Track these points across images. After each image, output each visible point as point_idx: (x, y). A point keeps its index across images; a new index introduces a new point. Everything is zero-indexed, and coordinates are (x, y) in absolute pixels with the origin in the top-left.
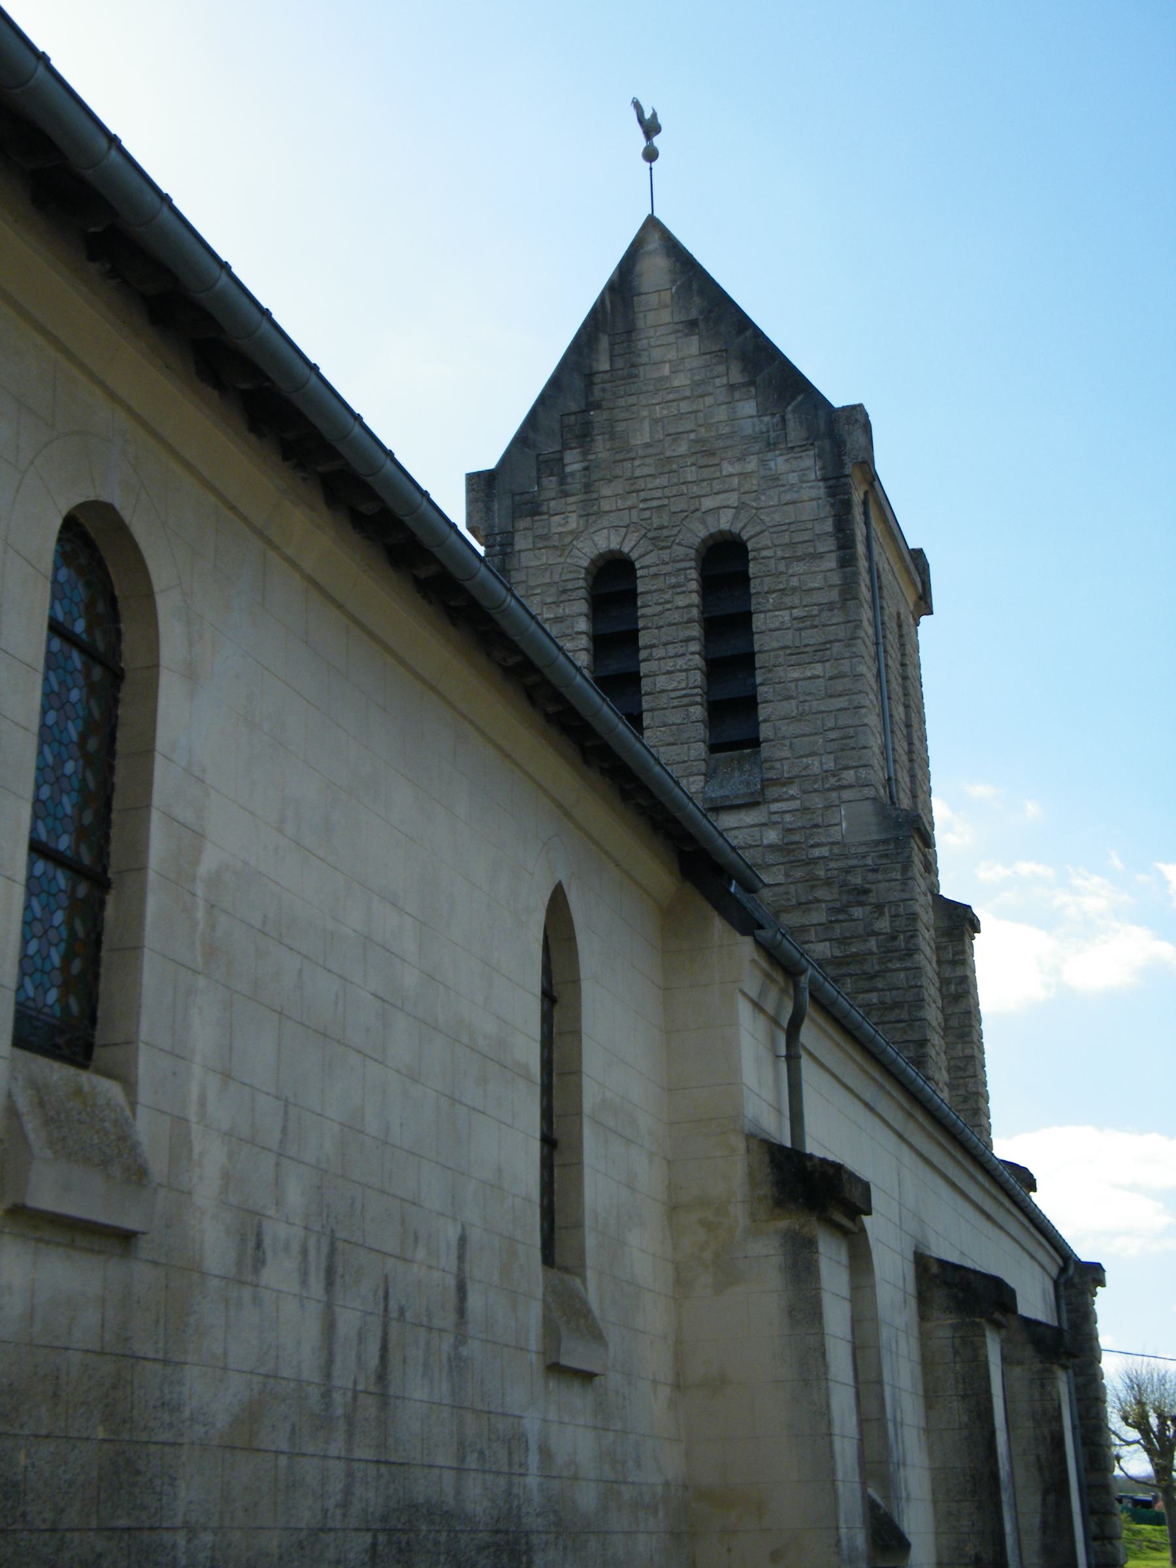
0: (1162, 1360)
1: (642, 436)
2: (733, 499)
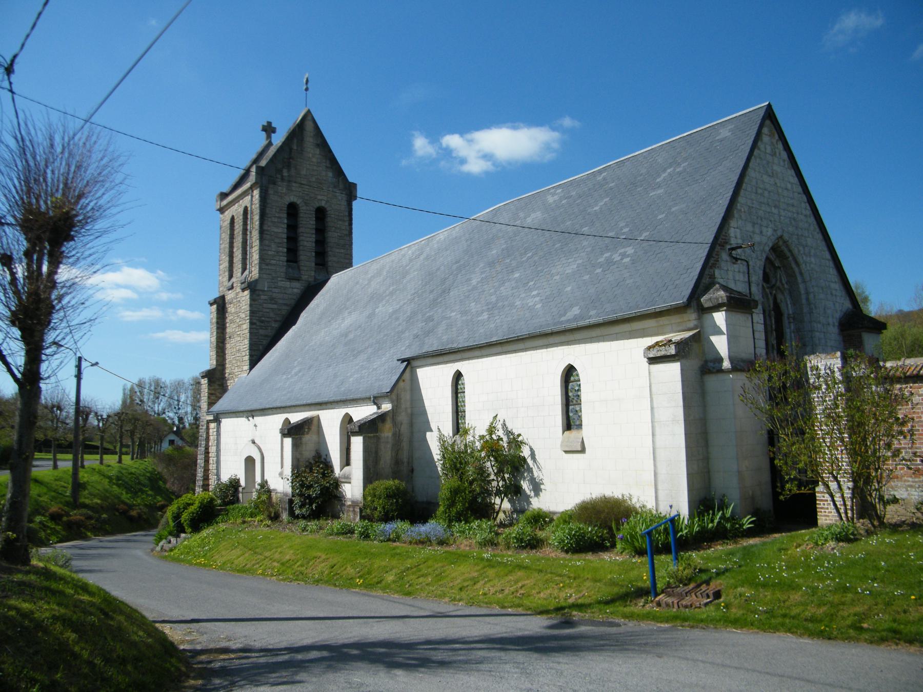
0: (660, 487)
1: (304, 172)
2: (325, 198)
